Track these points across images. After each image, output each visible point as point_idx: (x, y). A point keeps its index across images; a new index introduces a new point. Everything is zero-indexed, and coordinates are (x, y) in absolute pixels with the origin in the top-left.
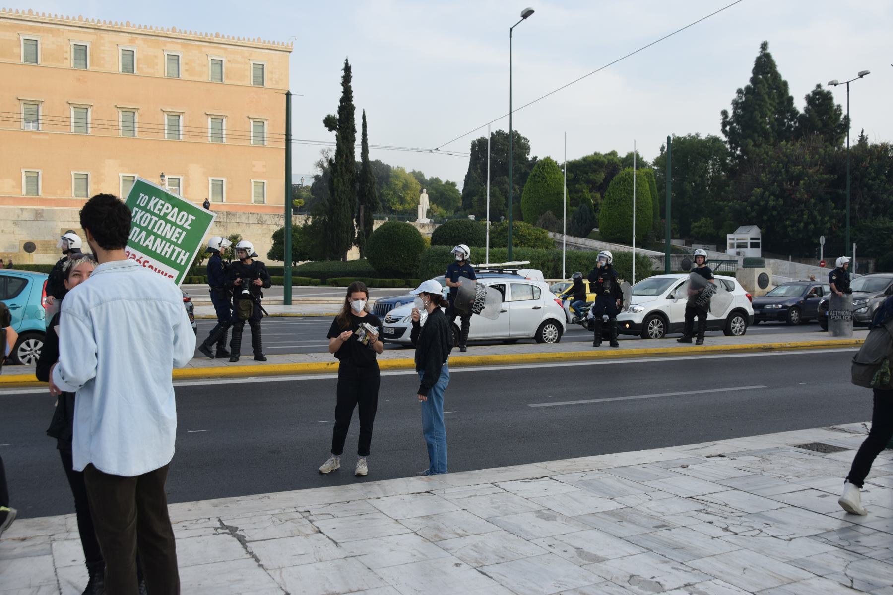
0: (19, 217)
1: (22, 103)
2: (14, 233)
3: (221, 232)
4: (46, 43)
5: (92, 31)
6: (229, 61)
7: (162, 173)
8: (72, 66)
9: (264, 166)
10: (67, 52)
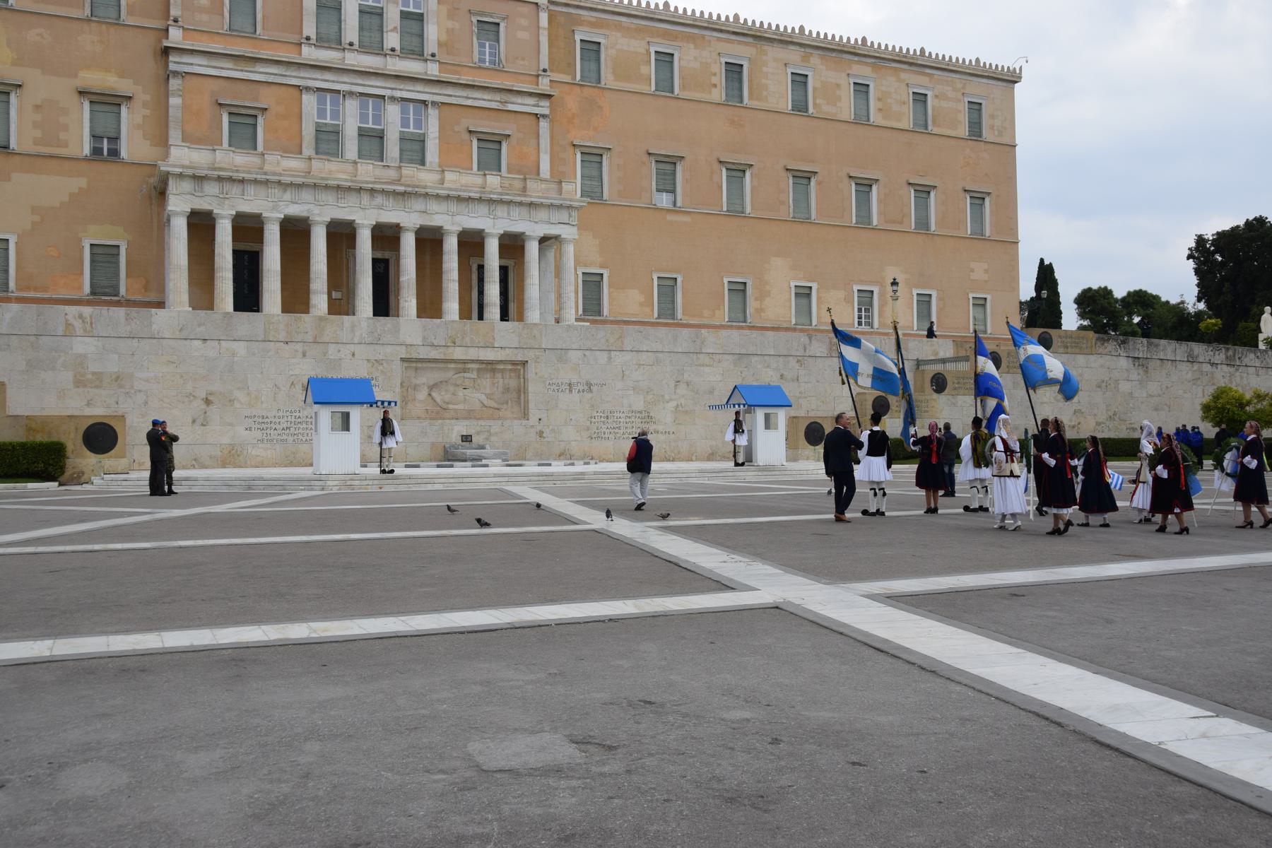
0: (805, 350)
1: (653, 159)
2: (798, 380)
3: (1140, 377)
4: (686, 58)
5: (750, 40)
6: (936, 97)
7: (895, 279)
8: (724, 98)
9: (986, 271)
10: (715, 74)
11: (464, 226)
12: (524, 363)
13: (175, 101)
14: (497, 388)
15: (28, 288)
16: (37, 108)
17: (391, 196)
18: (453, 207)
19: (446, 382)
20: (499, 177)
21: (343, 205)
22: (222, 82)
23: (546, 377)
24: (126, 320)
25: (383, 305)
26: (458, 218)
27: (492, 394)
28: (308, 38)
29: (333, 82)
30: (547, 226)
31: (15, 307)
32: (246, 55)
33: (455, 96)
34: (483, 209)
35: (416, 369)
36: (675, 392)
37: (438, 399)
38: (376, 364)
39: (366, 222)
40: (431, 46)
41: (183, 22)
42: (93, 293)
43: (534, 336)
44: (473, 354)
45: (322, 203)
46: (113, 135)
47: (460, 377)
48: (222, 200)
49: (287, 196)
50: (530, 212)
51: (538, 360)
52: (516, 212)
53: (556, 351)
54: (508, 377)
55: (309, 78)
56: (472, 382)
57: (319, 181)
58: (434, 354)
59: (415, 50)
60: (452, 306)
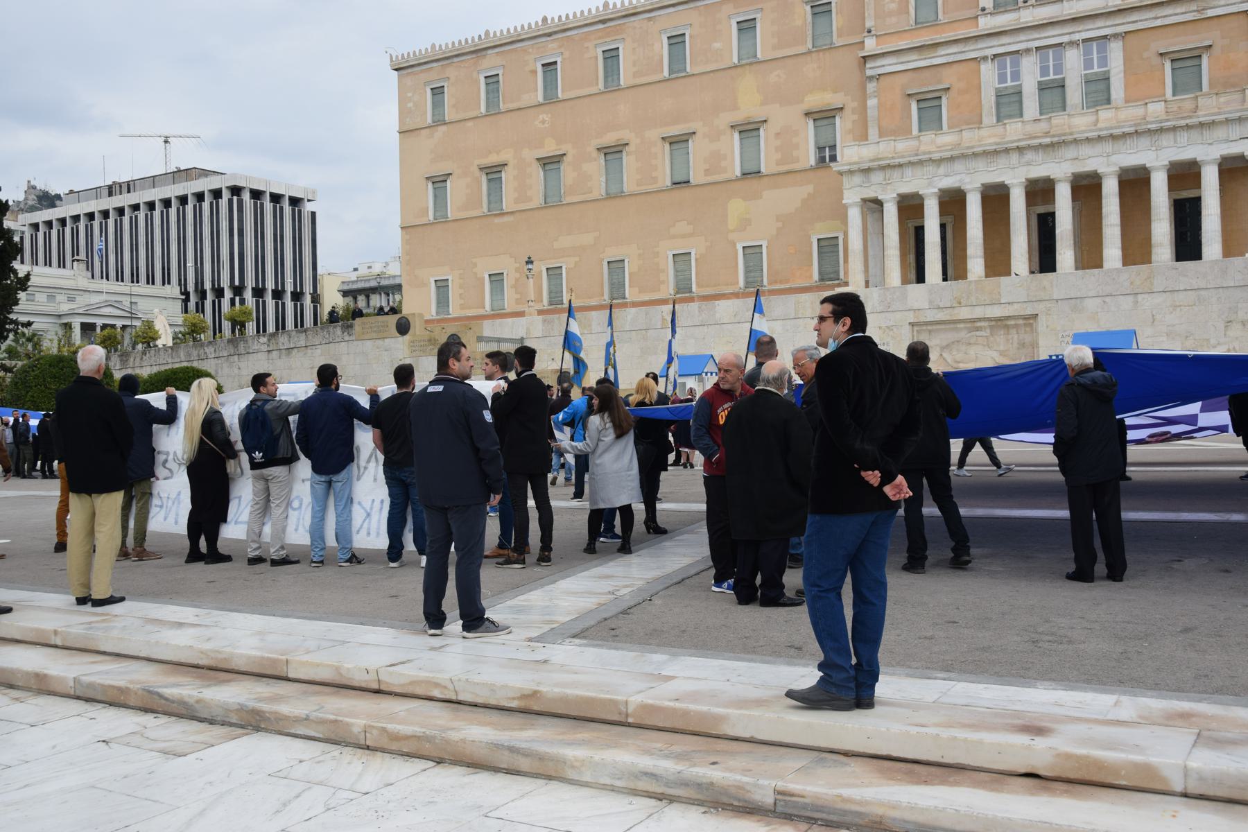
11: (1122, 165)
12: (1035, 316)
13: (872, 102)
14: (1012, 344)
15: (776, 282)
16: (778, 134)
17: (1040, 150)
18: (1108, 147)
19: (958, 341)
20: (1163, 103)
21: (992, 169)
22: (909, 73)
23: (1059, 329)
24: (699, 311)
25: (1045, 260)
26: (1114, 158)
27: (1006, 350)
28: (983, 9)
29: (1009, 44)
30: (1225, 145)
31: (633, 310)
32: (927, 43)
33: (1141, 21)
34: (1144, 142)
35: (930, 331)
36: (1225, 335)
37: (949, 360)
38: (887, 330)
39: (1015, 181)
41: (875, 30)
42: (822, 280)
43: (1044, 288)
44: (978, 312)
45: (972, 171)
46: (832, 144)
47: (973, 336)
48: (885, 186)
49: (942, 170)
50: (1202, 133)
51: (1049, 312)
52: (1183, 137)
53: (1070, 301)
54: (1023, 332)
55: (987, 48)
56: (986, 340)
57: (965, 151)
58: (940, 316)
60: (976, 265)
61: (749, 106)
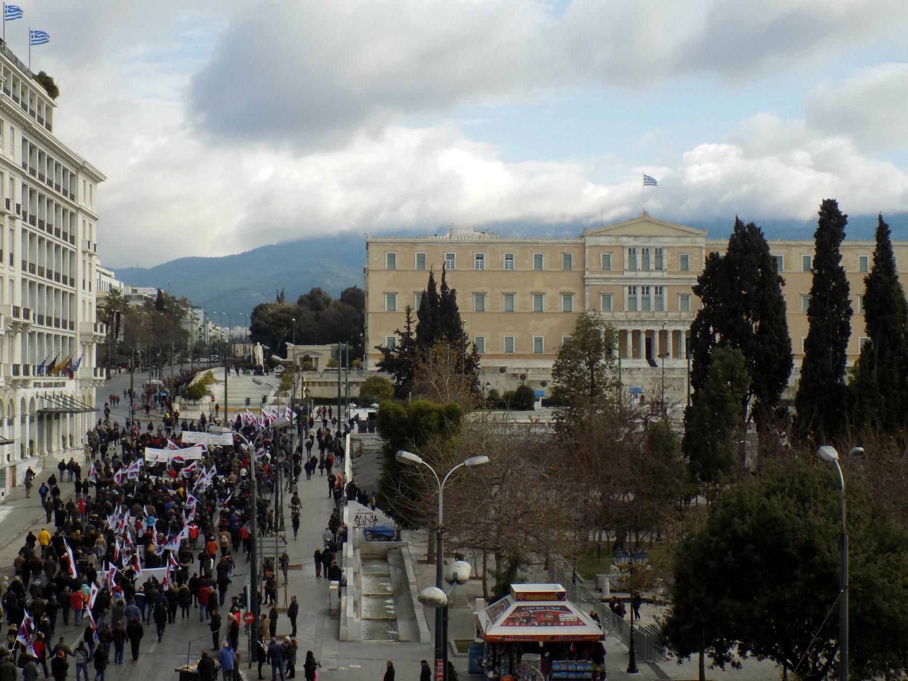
13: (587, 294)
40: (665, 266)
59: (659, 268)
61: (538, 285)
